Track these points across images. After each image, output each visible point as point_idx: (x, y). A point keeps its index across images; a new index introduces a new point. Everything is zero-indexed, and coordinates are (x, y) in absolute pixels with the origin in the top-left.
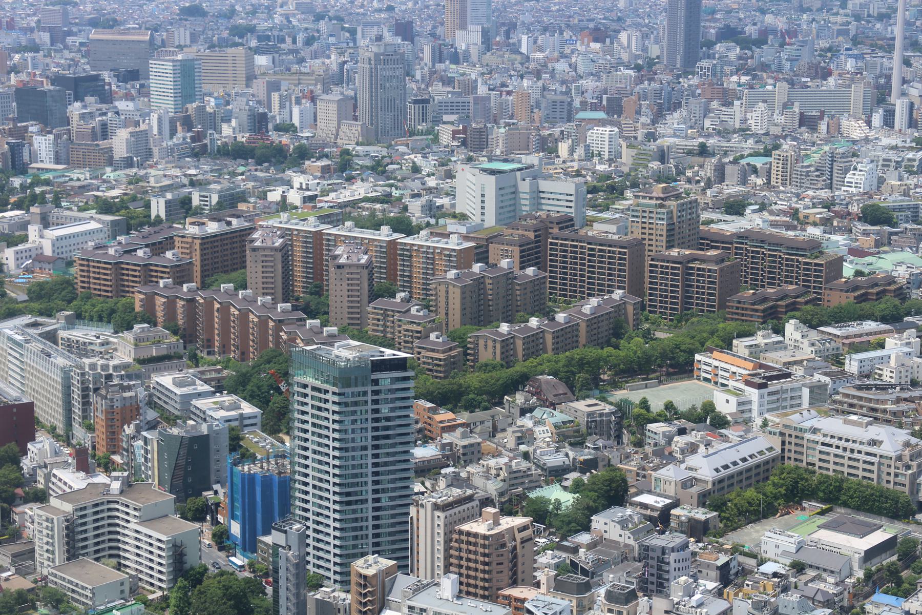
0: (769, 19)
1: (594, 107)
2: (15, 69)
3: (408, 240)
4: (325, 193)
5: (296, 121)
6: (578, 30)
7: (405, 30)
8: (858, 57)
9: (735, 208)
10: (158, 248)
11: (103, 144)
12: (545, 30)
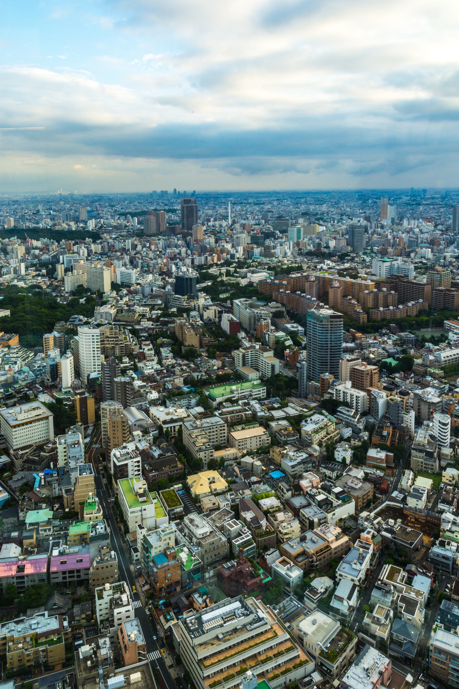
1: (425, 243)
2: (253, 230)
6: (423, 219)
11: (273, 251)
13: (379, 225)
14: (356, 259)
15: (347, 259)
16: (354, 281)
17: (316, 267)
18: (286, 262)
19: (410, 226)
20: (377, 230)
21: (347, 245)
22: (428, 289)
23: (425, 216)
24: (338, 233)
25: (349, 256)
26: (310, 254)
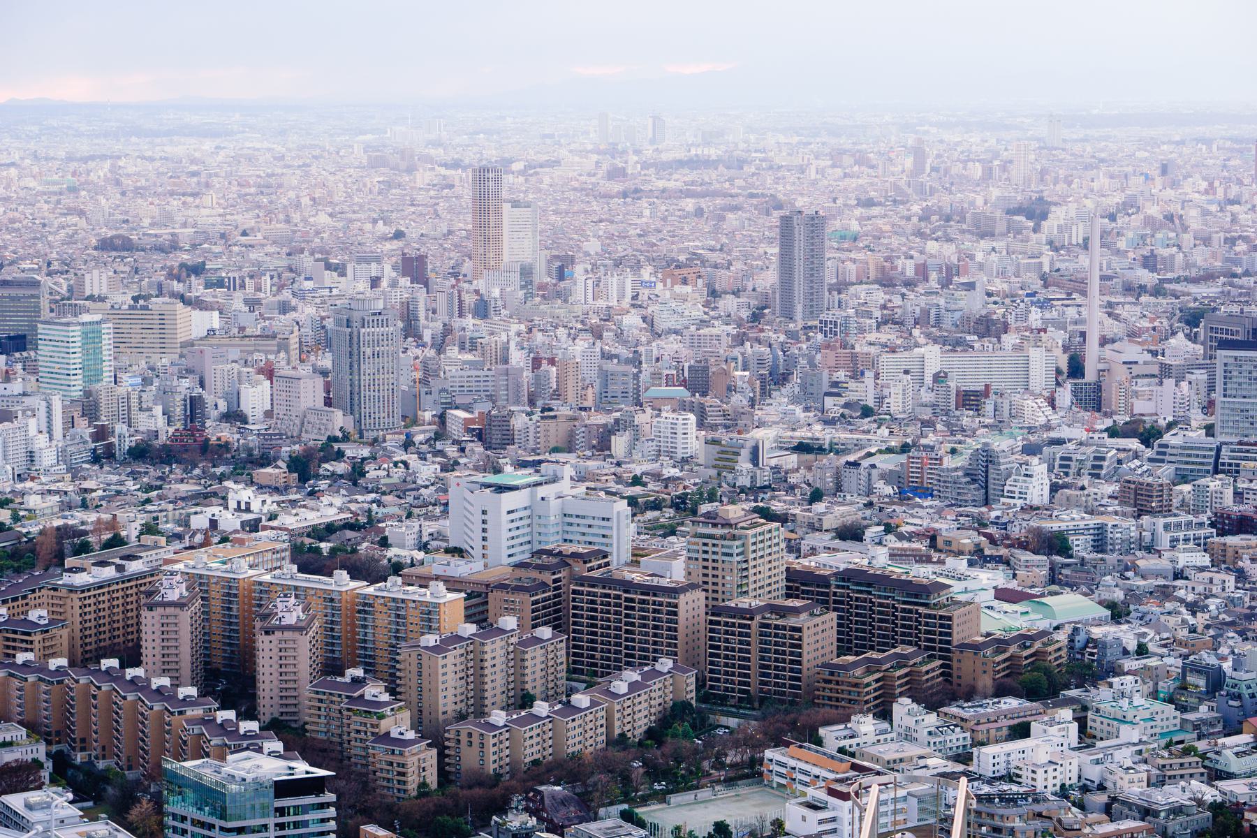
0: (932, 246)
1: (669, 381)
3: (371, 590)
8: (1045, 304)
12: (618, 263)
13: (469, 299)
14: (372, 472)
15: (334, 477)
18: (33, 501)
19: (602, 303)
20: (457, 323)
21: (328, 402)
22: (692, 606)
23: (663, 248)
24: (284, 346)
25: (340, 455)
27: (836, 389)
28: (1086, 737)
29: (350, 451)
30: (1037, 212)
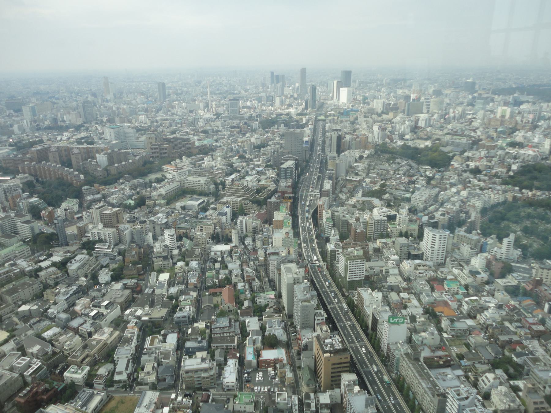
3: (91, 146)
4: (72, 136)
5: (65, 119)
7: (94, 95)
8: (202, 96)
9: (174, 132)
10: (24, 154)
11: (10, 129)
14: (90, 129)
16: (91, 146)
17: (56, 139)
26: (48, 128)
27: (169, 111)
28: (213, 160)
29: (86, 125)
30: (200, 82)
